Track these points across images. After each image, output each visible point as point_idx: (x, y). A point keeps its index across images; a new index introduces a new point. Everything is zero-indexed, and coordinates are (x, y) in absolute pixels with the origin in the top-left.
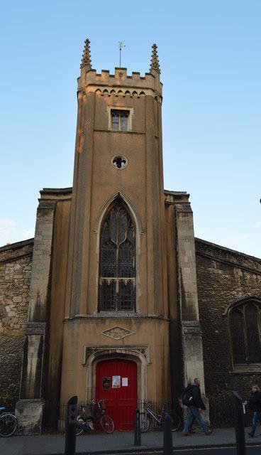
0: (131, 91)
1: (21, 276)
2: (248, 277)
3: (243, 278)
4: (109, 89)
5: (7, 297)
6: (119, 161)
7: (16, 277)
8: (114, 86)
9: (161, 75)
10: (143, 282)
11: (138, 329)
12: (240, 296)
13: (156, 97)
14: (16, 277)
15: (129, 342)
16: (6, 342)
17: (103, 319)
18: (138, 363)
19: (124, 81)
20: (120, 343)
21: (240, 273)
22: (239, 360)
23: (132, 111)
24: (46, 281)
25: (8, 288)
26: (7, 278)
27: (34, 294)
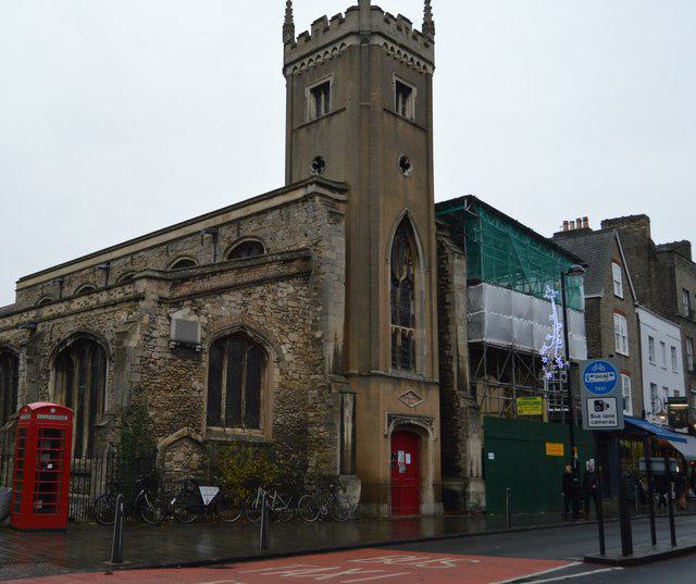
1: (295, 304)
5: (282, 331)
6: (404, 165)
7: (290, 303)
8: (402, 46)
9: (436, 45)
10: (423, 335)
11: (427, 393)
14: (290, 303)
16: (285, 397)
17: (399, 379)
18: (423, 438)
19: (400, 38)
20: (413, 413)
23: (414, 90)
24: (342, 320)
25: (281, 319)
26: (280, 304)
27: (331, 336)
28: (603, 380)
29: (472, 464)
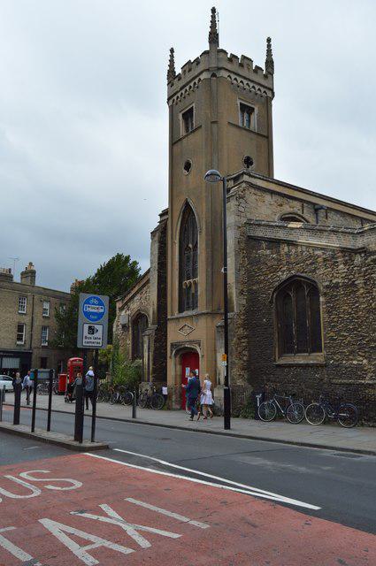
0: (192, 84)
2: (294, 251)
3: (288, 255)
4: (179, 95)
8: (181, 89)
12: (284, 277)
13: (214, 75)
15: (192, 337)
20: (187, 339)
21: (286, 249)
22: (287, 349)
28: (96, 311)
29: (219, 374)
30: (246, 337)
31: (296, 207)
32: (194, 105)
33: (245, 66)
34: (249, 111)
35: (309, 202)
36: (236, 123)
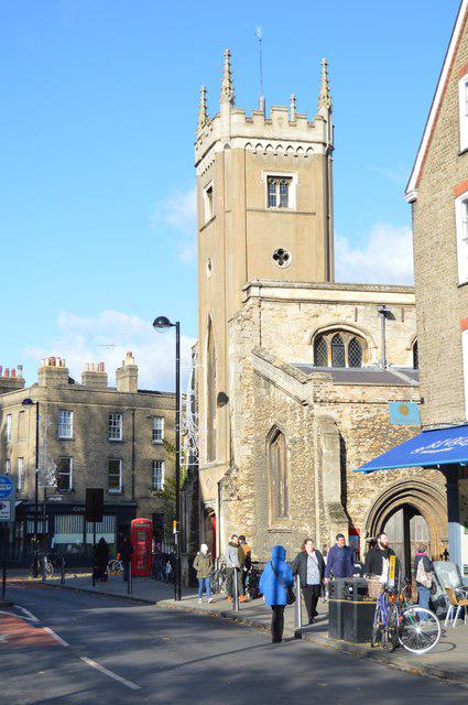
12: (272, 424)
13: (227, 146)
30: (252, 495)
31: (341, 316)
32: (212, 184)
33: (275, 122)
34: (285, 181)
35: (366, 303)
36: (259, 207)
